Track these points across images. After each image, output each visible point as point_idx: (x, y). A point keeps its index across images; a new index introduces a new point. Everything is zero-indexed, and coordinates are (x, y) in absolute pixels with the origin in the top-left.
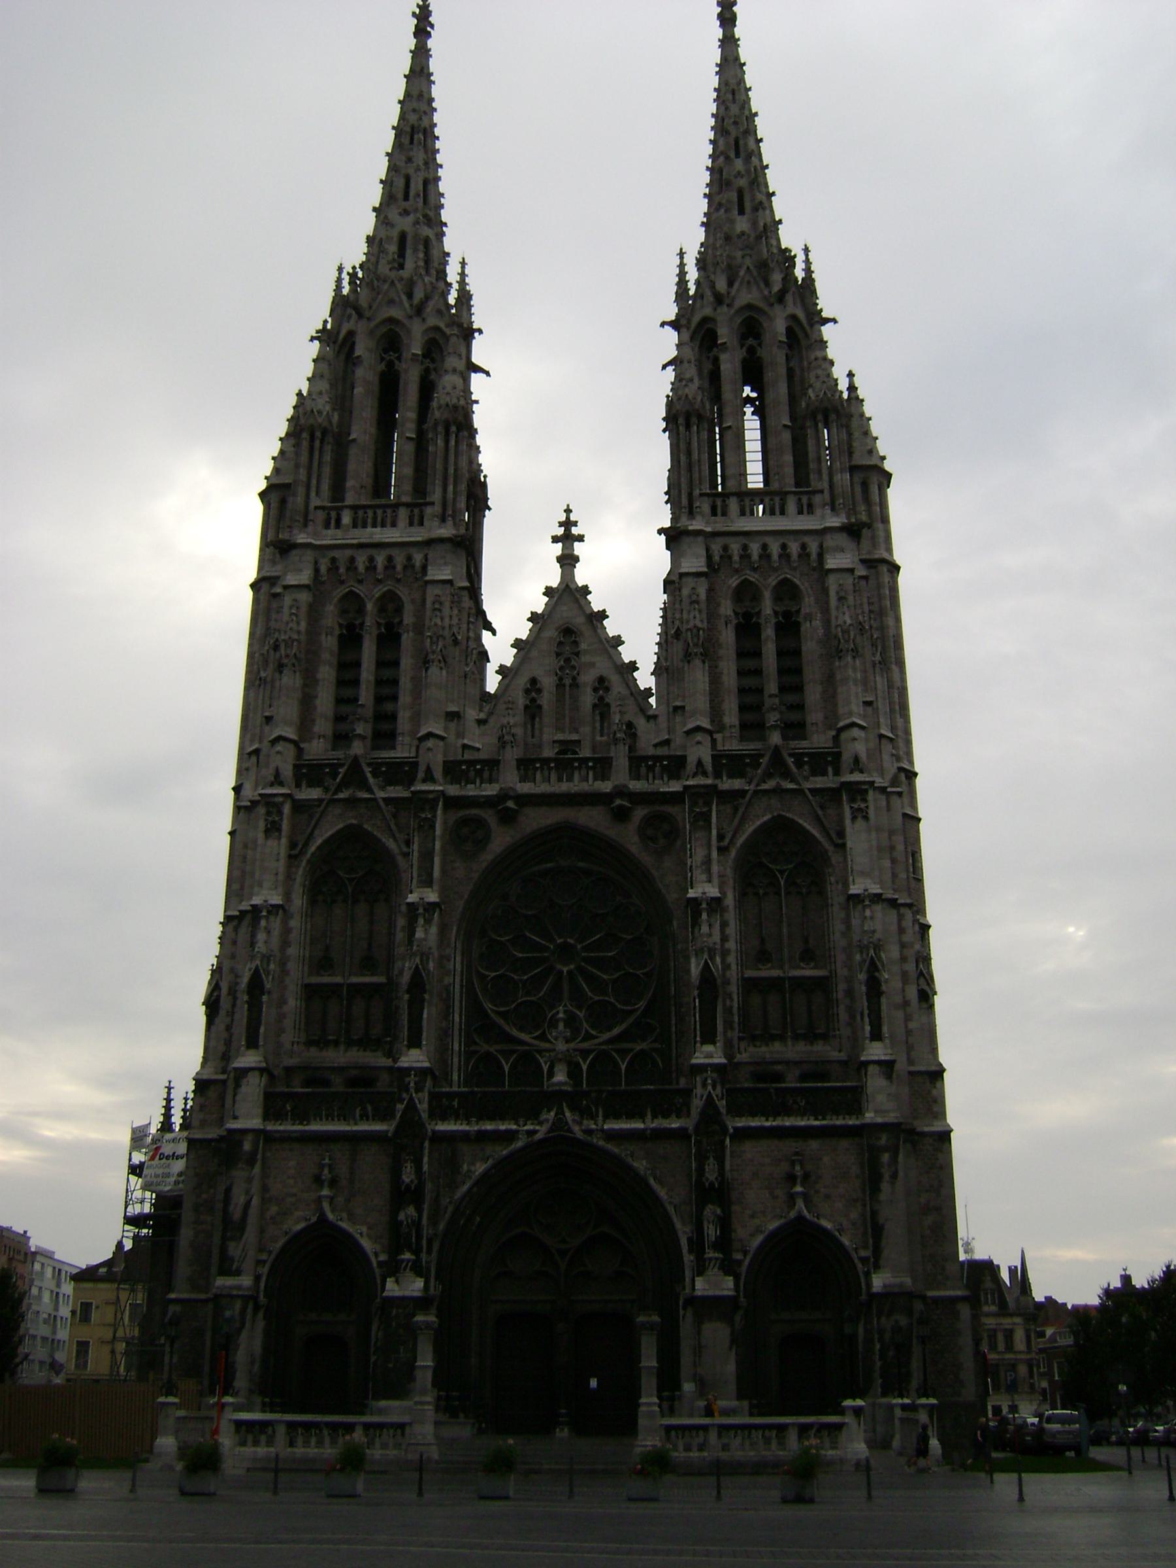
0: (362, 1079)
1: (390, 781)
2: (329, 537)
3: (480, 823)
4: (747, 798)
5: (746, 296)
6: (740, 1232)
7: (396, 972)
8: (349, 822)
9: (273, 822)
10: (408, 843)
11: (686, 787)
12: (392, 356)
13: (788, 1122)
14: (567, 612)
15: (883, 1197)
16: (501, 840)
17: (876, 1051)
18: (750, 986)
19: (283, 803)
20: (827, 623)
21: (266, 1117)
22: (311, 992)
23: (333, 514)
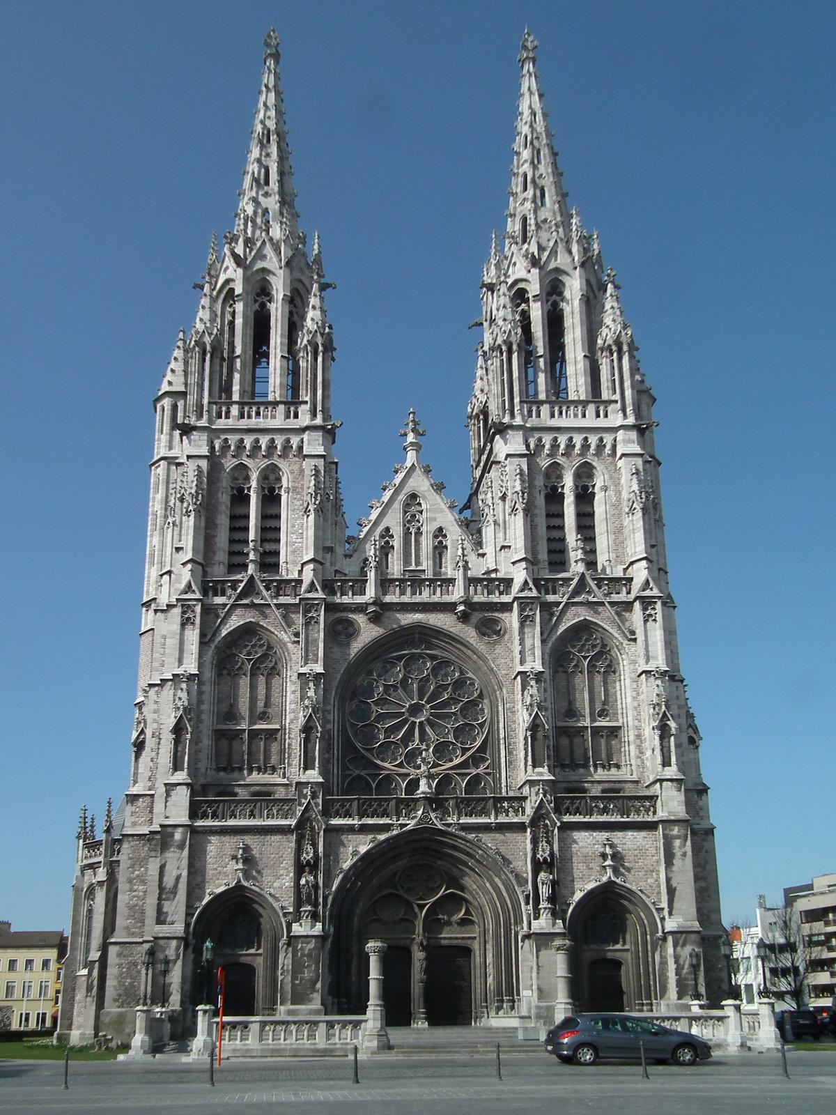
2: (221, 423)
3: (351, 623)
4: (561, 607)
7: (288, 721)
8: (248, 620)
9: (189, 619)
10: (297, 635)
11: (515, 599)
12: (265, 299)
15: (675, 868)
16: (367, 633)
19: (194, 606)
21: (193, 815)
23: (224, 409)
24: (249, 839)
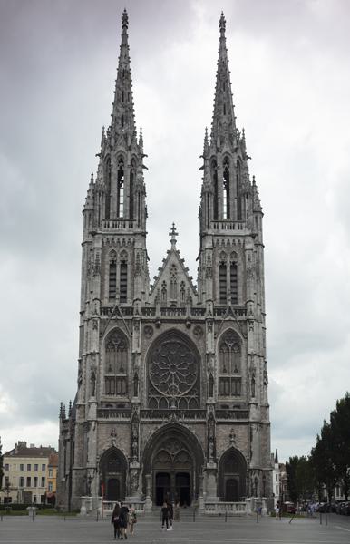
0: (121, 406)
1: (127, 314)
3: (151, 328)
5: (226, 149)
6: (218, 451)
13: (231, 420)
14: (173, 260)
17: (253, 401)
18: (221, 379)
20: (245, 266)
21: (98, 417)
22: (106, 378)
24: (115, 426)
